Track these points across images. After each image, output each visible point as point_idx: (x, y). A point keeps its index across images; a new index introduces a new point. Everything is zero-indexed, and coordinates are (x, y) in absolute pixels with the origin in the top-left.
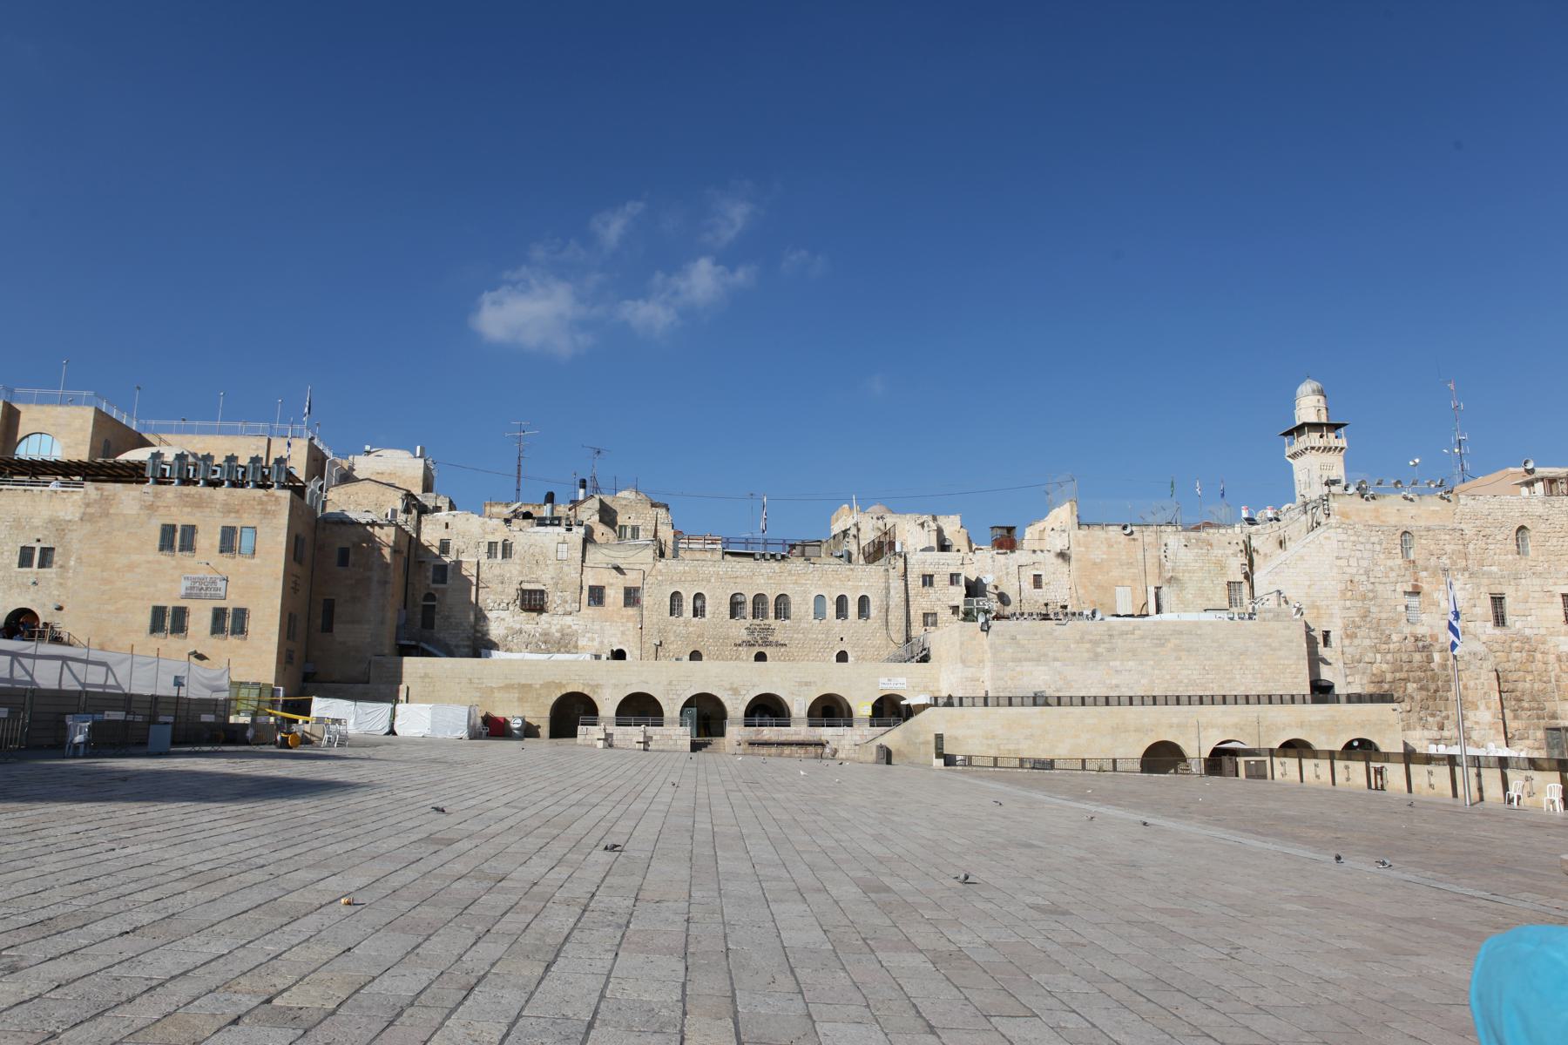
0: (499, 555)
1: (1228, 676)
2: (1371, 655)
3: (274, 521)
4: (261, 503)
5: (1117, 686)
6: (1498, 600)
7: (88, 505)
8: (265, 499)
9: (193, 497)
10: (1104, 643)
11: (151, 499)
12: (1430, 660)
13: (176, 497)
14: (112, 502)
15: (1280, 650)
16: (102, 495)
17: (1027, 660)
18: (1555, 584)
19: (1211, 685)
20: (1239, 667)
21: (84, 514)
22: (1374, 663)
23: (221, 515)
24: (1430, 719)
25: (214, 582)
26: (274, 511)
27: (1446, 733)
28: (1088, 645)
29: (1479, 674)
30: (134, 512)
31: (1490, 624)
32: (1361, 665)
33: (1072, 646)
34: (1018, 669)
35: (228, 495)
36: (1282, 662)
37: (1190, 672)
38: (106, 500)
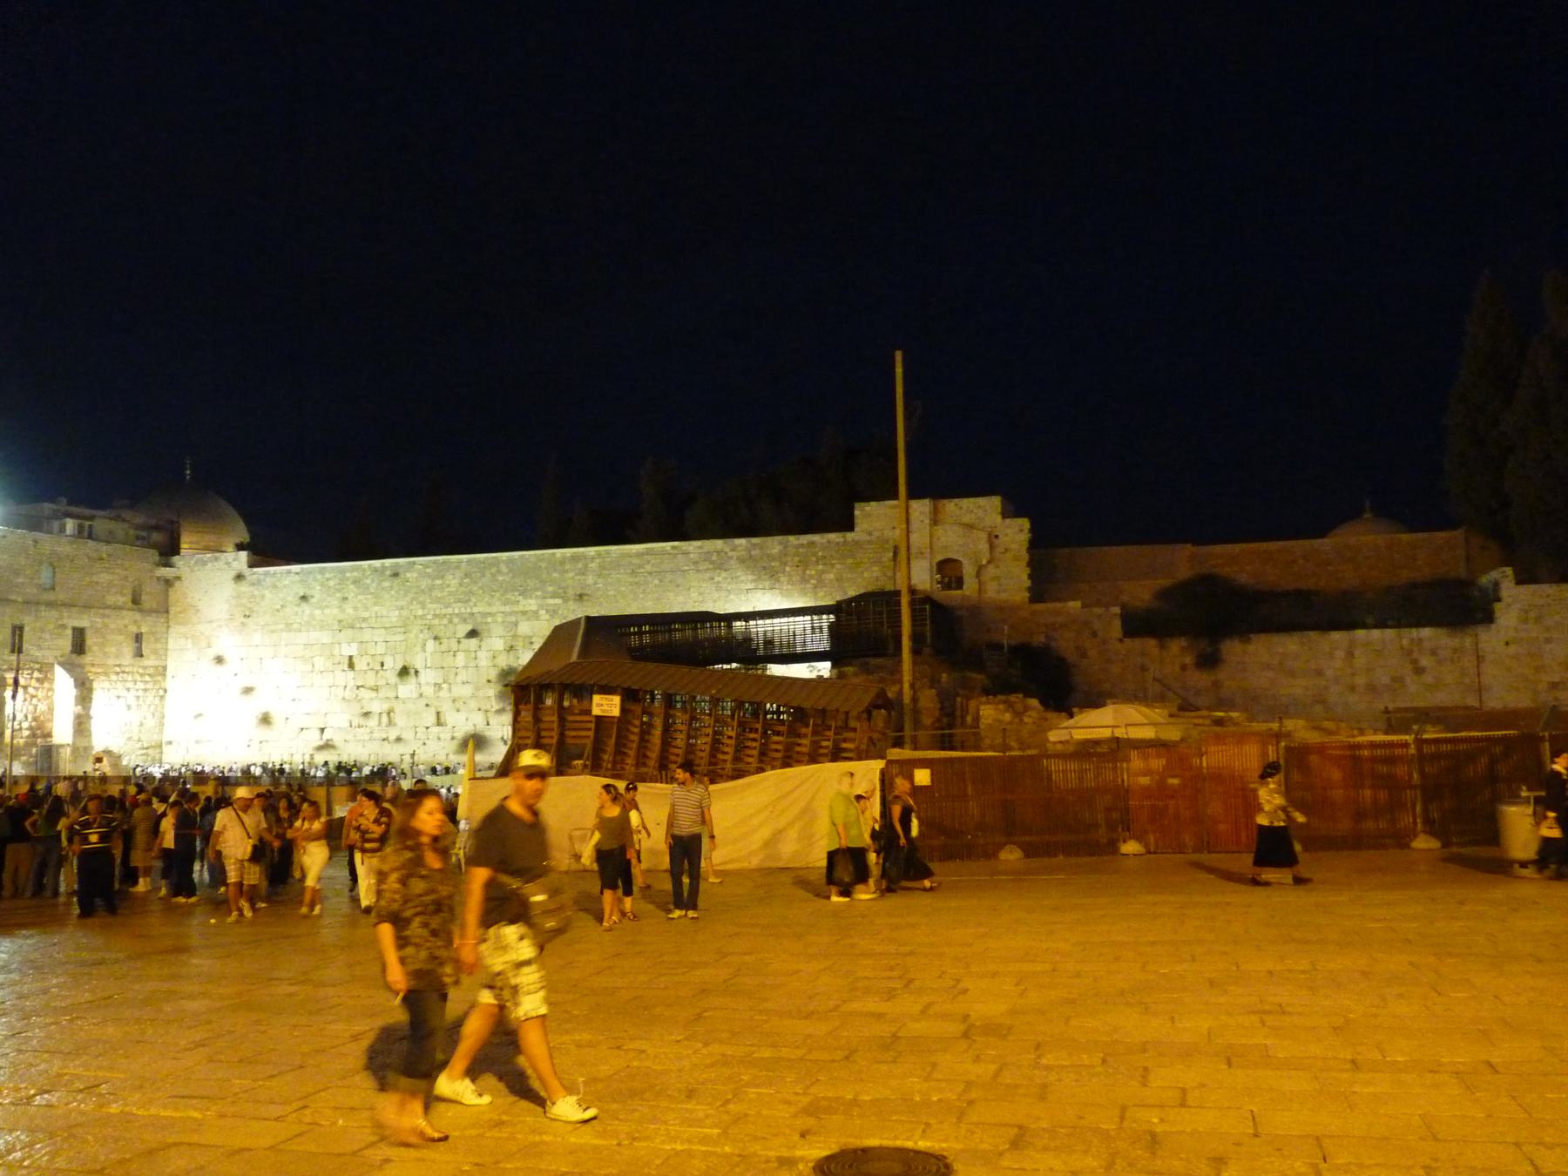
6: (18, 630)
18: (69, 617)
31: (7, 651)
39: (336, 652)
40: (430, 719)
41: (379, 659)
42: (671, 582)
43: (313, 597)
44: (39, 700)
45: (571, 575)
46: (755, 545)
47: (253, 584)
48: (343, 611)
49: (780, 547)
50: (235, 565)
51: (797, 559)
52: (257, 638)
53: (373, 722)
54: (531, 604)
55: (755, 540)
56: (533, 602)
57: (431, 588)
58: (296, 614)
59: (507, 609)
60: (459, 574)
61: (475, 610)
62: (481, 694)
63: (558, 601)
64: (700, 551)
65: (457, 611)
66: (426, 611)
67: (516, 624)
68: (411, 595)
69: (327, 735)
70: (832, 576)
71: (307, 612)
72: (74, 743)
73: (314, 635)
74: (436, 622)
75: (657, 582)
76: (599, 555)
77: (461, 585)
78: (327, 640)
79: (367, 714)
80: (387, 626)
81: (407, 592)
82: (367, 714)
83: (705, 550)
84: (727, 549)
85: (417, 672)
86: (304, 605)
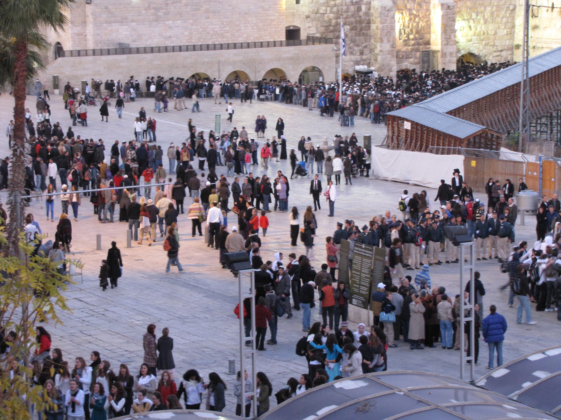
1: (237, 28)
2: (324, 8)
5: (170, 37)
10: (162, 9)
12: (359, 9)
15: (269, 10)
17: (115, 22)
19: (227, 34)
20: (243, 22)
22: (326, 13)
24: (356, 48)
27: (364, 57)
28: (153, 11)
29: (386, 20)
32: (318, 15)
33: (143, 11)
34: (109, 28)
36: (270, 18)
37: (214, 26)
44: (420, 19)
72: (442, 50)
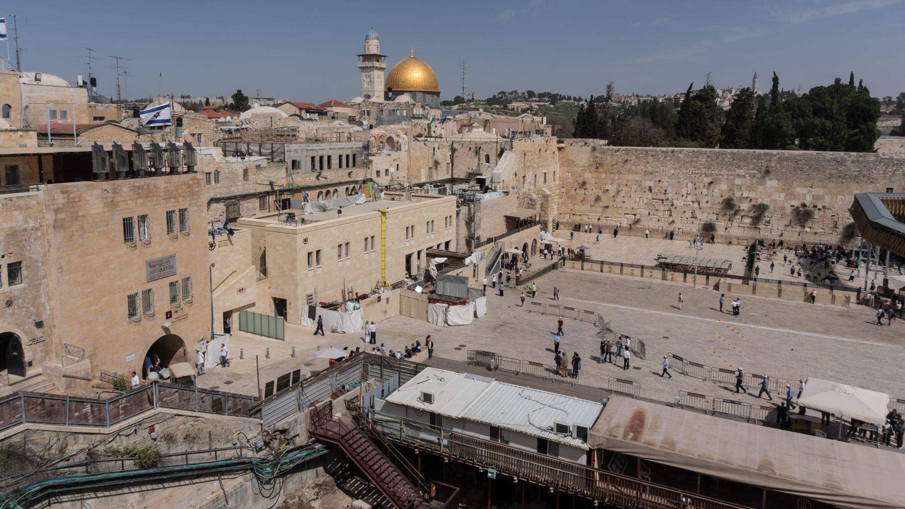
0: (213, 182)
3: (199, 200)
4: (189, 186)
7: (57, 211)
8: (191, 182)
9: (143, 188)
11: (111, 195)
13: (131, 190)
14: (79, 204)
16: (68, 197)
21: (56, 221)
23: (164, 201)
25: (169, 261)
26: (198, 192)
30: (99, 211)
35: (166, 183)
38: (73, 202)
39: (643, 184)
40: (689, 214)
41: (665, 189)
42: (815, 168)
43: (631, 161)
45: (763, 161)
46: (861, 156)
47: (601, 153)
48: (646, 167)
49: (874, 158)
50: (592, 144)
51: (883, 164)
52: (603, 176)
53: (660, 214)
54: (742, 172)
55: (861, 154)
56: (743, 171)
57: (692, 162)
58: (623, 167)
59: (730, 173)
60: (705, 156)
61: (713, 172)
62: (714, 207)
63: (757, 172)
64: (831, 156)
65: (704, 172)
66: (688, 171)
67: (734, 179)
68: (681, 163)
69: (638, 217)
70: (900, 172)
71: (629, 166)
73: (632, 177)
74: (693, 175)
75: (808, 168)
76: (778, 154)
77: (706, 161)
78: (638, 179)
79: (657, 210)
80: (669, 175)
81: (679, 162)
82: (657, 210)
83: (834, 156)
84: (846, 157)
85: (682, 196)
86: (627, 163)
